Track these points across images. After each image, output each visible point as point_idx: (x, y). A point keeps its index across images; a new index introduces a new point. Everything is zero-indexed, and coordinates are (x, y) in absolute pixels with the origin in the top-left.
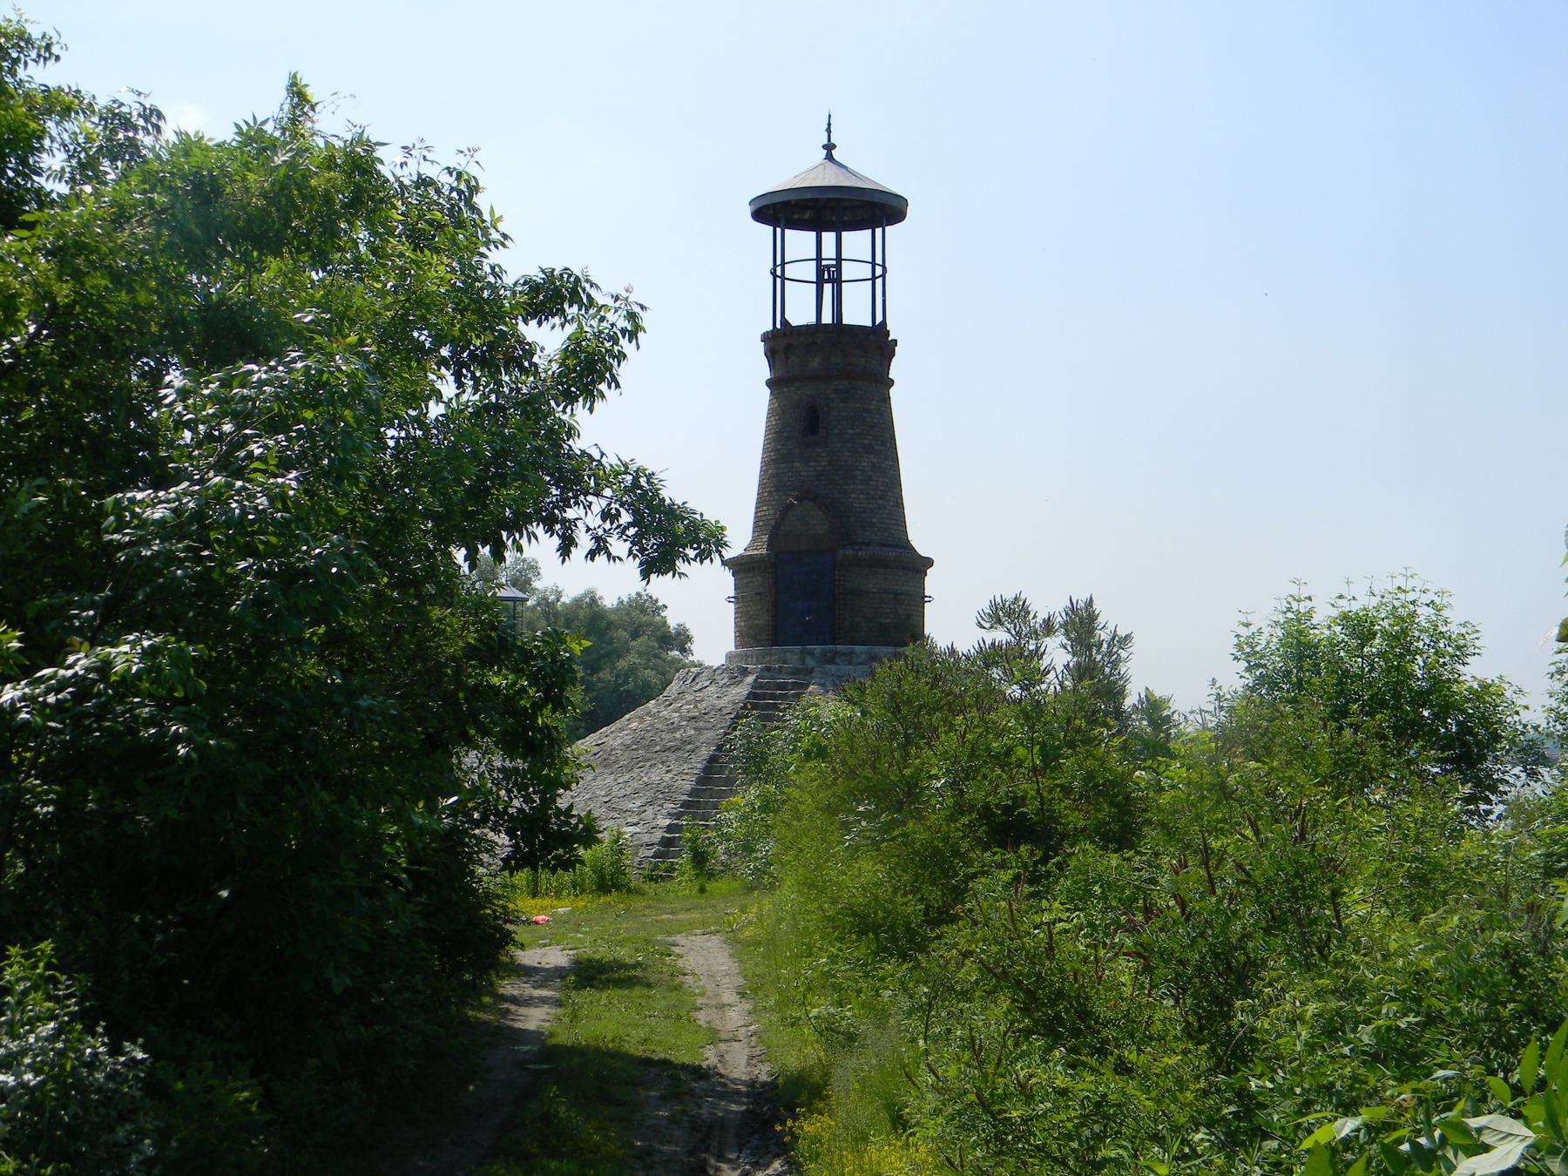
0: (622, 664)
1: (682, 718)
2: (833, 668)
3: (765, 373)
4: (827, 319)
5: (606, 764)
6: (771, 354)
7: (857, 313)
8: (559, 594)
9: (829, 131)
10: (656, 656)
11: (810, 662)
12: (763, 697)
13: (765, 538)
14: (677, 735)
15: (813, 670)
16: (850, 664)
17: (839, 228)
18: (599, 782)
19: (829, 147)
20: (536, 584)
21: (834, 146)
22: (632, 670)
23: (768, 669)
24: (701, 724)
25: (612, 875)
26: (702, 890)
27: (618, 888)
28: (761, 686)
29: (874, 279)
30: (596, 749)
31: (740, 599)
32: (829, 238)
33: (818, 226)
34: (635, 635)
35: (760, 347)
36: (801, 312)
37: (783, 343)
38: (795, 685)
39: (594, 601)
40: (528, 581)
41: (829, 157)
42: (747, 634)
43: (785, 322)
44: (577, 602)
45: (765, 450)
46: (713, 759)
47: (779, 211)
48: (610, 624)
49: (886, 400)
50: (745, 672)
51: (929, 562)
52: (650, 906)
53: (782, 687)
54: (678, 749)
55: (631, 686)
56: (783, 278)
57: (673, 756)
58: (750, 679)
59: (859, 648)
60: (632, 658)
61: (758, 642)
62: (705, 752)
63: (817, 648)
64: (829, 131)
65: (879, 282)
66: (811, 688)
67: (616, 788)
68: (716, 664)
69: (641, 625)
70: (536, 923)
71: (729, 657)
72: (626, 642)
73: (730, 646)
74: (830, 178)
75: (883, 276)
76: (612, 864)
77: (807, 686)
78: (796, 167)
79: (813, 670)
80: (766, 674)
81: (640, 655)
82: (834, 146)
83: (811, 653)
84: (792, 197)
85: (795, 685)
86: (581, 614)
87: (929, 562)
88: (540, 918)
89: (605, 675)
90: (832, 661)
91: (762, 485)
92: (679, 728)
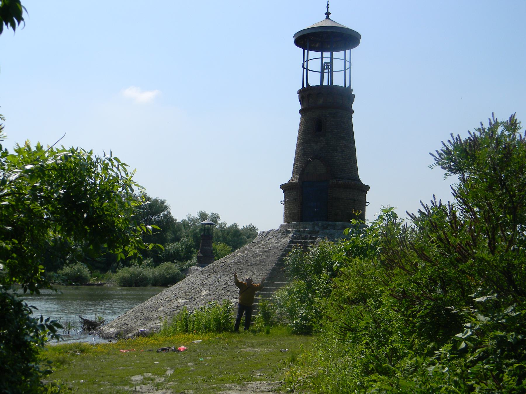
1: (260, 251)
2: (327, 231)
3: (299, 107)
4: (325, 83)
5: (226, 270)
6: (301, 100)
7: (338, 81)
8: (225, 225)
9: (328, 7)
11: (317, 229)
12: (296, 243)
13: (298, 176)
14: (258, 259)
15: (318, 232)
16: (334, 229)
17: (332, 50)
18: (222, 278)
19: (328, 14)
20: (219, 222)
21: (330, 14)
23: (298, 231)
24: (269, 254)
25: (224, 323)
26: (268, 333)
27: (226, 329)
28: (296, 238)
29: (345, 70)
30: (222, 264)
31: (301, 123)
32: (327, 55)
33: (321, 49)
35: (297, 96)
36: (314, 80)
37: (307, 94)
38: (310, 238)
39: (236, 226)
40: (216, 221)
41: (328, 18)
42: (289, 216)
43: (308, 85)
44: (231, 227)
45: (298, 139)
46: (273, 270)
47: (308, 40)
48: (241, 234)
49: (351, 118)
50: (288, 232)
51: (367, 188)
52: (240, 341)
53: (305, 238)
54: (258, 265)
56: (308, 70)
57: (256, 268)
58: (291, 235)
59: (338, 223)
61: (294, 220)
62: (270, 266)
63: (320, 223)
64: (328, 7)
65: (348, 72)
66: (318, 239)
67: (229, 282)
68: (276, 227)
69: (250, 235)
70: (179, 351)
71: (281, 226)
72: (245, 240)
73: (282, 222)
74: (328, 24)
75: (350, 68)
76: (224, 317)
77: (316, 238)
78: (314, 19)
79: (318, 232)
80: (298, 233)
82: (330, 14)
83: (317, 225)
84: (313, 31)
85: (310, 238)
87: (367, 188)
88: (182, 347)
90: (327, 228)
91: (297, 154)
92: (258, 255)
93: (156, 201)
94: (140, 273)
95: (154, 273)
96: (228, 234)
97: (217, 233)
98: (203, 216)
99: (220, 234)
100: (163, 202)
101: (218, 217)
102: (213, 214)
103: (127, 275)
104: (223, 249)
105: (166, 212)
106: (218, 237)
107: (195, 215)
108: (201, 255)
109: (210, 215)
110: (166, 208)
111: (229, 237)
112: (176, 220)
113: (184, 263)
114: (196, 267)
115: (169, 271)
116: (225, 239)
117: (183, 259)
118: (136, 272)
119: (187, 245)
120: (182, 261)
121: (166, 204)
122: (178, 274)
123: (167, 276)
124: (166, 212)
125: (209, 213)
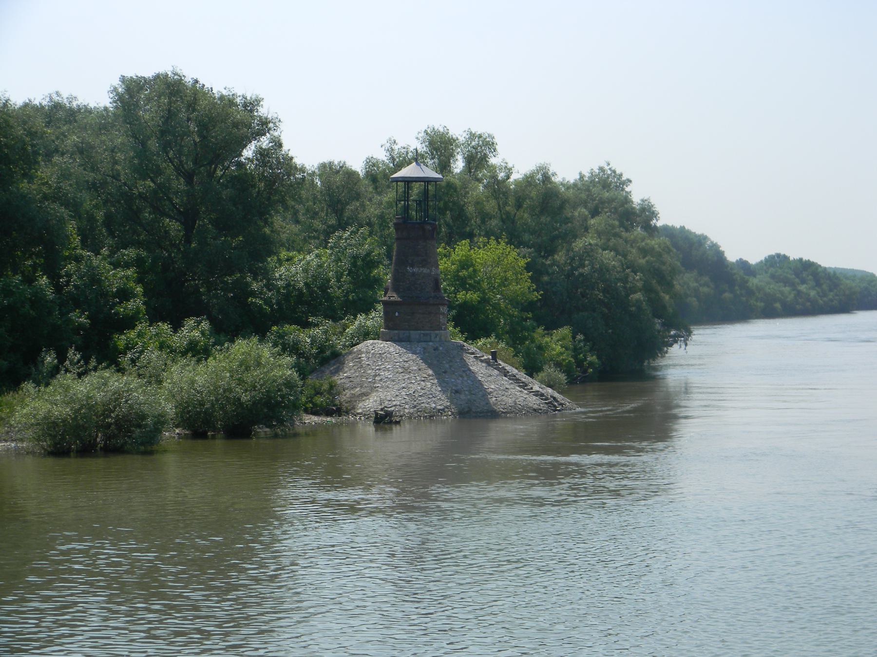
0: (579, 244)
8: (509, 172)
10: (616, 235)
20: (493, 161)
22: (589, 252)
34: (595, 213)
39: (546, 178)
40: (485, 158)
44: (529, 181)
48: (564, 202)
55: (586, 270)
60: (590, 239)
69: (602, 202)
72: (585, 220)
81: (599, 234)
86: (534, 194)
89: (560, 257)
93: (228, 102)
94: (118, 395)
95: (193, 382)
96: (519, 206)
98: (440, 146)
99: (491, 206)
100: (251, 106)
101: (489, 144)
102: (472, 136)
104: (498, 263)
105: (265, 142)
106: (485, 217)
107: (412, 141)
108: (395, 297)
109: (462, 139)
110: (265, 126)
111: (525, 217)
113: (345, 327)
114: (381, 345)
115: (248, 378)
116: (508, 220)
118: (99, 396)
119: (355, 258)
120: (335, 319)
121: (263, 111)
122: (289, 384)
123: (245, 398)
124: (265, 142)
125: (458, 132)
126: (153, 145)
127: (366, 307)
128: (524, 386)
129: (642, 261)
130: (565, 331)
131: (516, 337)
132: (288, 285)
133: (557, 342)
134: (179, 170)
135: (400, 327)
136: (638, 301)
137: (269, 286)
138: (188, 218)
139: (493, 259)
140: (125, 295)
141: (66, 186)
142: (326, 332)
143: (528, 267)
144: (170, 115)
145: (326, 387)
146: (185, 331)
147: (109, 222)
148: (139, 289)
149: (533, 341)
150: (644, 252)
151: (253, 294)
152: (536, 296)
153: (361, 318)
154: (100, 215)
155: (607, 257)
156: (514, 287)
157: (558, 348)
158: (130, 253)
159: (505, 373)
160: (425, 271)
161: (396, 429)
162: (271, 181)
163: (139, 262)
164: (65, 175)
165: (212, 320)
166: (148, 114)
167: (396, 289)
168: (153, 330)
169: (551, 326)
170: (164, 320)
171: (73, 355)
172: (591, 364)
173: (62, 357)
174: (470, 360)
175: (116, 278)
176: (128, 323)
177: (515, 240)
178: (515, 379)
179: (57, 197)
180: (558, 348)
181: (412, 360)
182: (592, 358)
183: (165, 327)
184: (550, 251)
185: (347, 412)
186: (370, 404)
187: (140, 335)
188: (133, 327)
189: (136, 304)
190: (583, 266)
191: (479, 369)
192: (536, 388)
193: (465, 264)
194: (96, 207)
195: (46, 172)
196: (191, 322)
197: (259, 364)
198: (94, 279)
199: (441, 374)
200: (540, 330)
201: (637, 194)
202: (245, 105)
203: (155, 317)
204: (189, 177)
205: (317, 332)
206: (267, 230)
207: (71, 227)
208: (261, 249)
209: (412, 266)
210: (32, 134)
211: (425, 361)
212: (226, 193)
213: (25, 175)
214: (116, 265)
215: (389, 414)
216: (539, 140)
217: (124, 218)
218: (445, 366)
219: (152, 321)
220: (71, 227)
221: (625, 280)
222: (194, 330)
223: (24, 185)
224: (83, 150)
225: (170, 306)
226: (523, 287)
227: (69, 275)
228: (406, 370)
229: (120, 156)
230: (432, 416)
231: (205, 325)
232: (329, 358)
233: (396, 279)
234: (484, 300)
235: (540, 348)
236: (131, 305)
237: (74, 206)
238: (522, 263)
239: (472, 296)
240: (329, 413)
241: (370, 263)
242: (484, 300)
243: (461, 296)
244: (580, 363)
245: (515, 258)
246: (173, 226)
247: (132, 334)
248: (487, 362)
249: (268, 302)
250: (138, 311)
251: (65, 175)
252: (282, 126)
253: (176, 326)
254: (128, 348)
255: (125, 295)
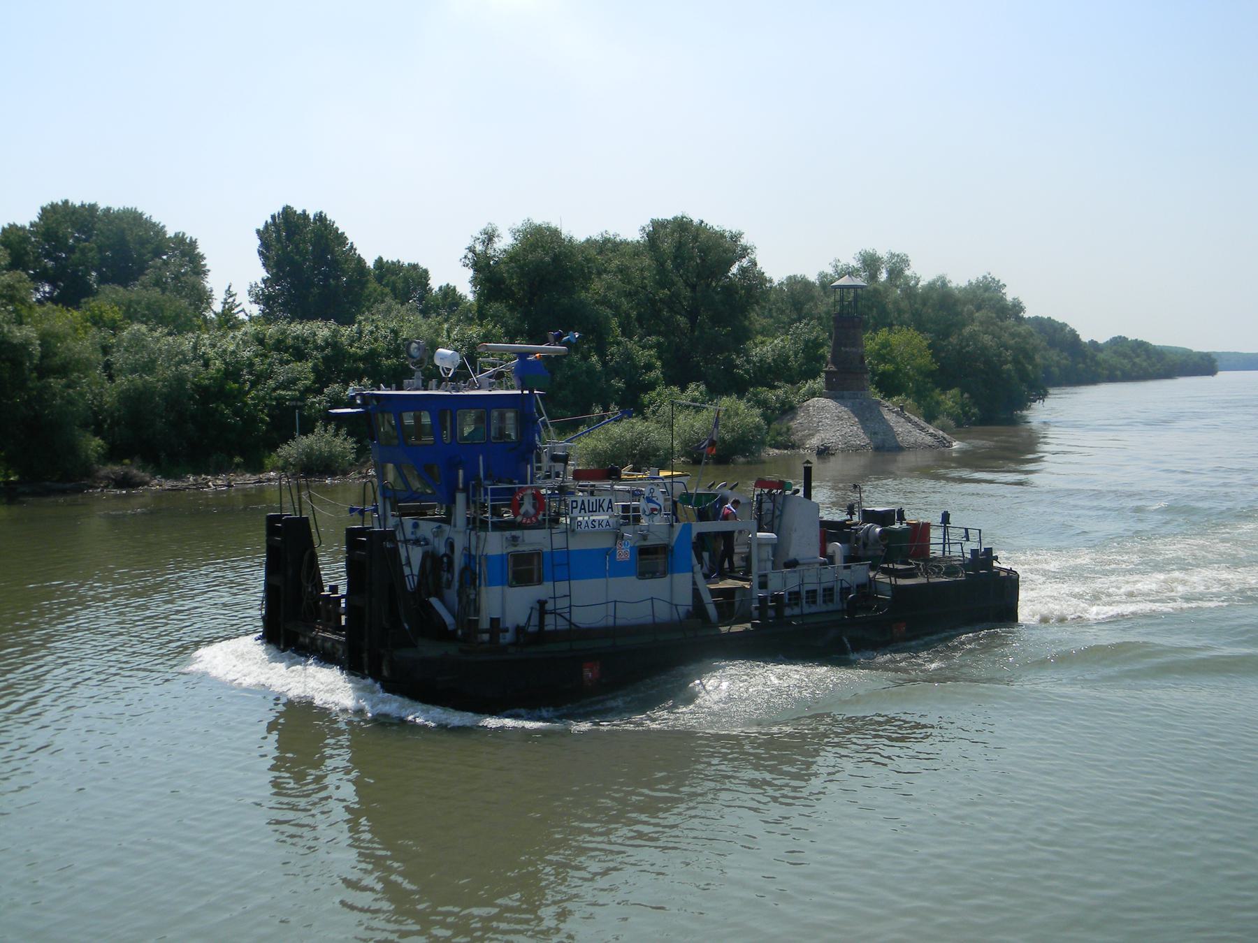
20: (907, 273)
22: (973, 336)
34: (979, 308)
39: (944, 284)
40: (902, 271)
44: (931, 287)
69: (983, 301)
72: (972, 313)
81: (981, 323)
86: (935, 296)
89: (954, 340)
95: (693, 426)
96: (924, 304)
97: (896, 302)
98: (870, 263)
99: (904, 304)
100: (735, 238)
101: (905, 261)
102: (893, 255)
103: (603, 446)
104: (908, 344)
106: (900, 312)
107: (851, 260)
108: (833, 368)
110: (745, 251)
112: (771, 281)
113: (800, 388)
114: (823, 401)
117: (794, 378)
119: (806, 342)
120: (793, 383)
121: (743, 242)
122: (758, 428)
123: (727, 437)
124: (745, 262)
125: (883, 253)
126: (669, 265)
127: (813, 375)
128: (922, 429)
129: (1012, 342)
130: (955, 391)
131: (920, 395)
132: (761, 361)
133: (949, 399)
134: (687, 284)
135: (835, 390)
136: (1009, 370)
137: (748, 362)
138: (692, 315)
139: (906, 343)
140: (649, 367)
141: (610, 294)
142: (786, 392)
143: (930, 347)
144: (680, 246)
145: (784, 429)
146: (689, 391)
147: (640, 319)
148: (659, 364)
149: (932, 398)
150: (1013, 335)
151: (737, 367)
152: (935, 367)
153: (810, 382)
154: (634, 314)
155: (987, 339)
156: (919, 361)
157: (950, 403)
158: (654, 339)
159: (910, 421)
160: (854, 350)
161: (832, 458)
162: (750, 289)
163: (658, 345)
164: (610, 288)
165: (707, 384)
166: (667, 245)
167: (834, 363)
168: (667, 391)
169: (946, 388)
170: (675, 385)
171: (614, 408)
172: (974, 415)
173: (606, 409)
174: (885, 412)
175: (643, 356)
176: (651, 386)
177: (921, 327)
178: (916, 425)
179: (605, 302)
180: (950, 403)
181: (844, 411)
182: (975, 410)
183: (676, 389)
184: (947, 336)
185: (799, 448)
186: (815, 441)
187: (659, 394)
188: (654, 389)
189: (656, 374)
190: (968, 345)
191: (891, 418)
192: (931, 431)
193: (885, 345)
194: (631, 308)
195: (597, 285)
196: (693, 386)
197: (737, 414)
198: (628, 357)
199: (863, 422)
200: (938, 391)
201: (1010, 295)
202: (731, 238)
203: (669, 381)
204: (693, 287)
205: (780, 392)
206: (747, 323)
207: (614, 322)
208: (742, 336)
209: (845, 346)
210: (588, 260)
211: (853, 412)
212: (717, 298)
213: (583, 288)
214: (644, 348)
215: (827, 448)
216: (941, 258)
217: (649, 315)
218: (867, 415)
219: (667, 385)
220: (614, 322)
221: (999, 355)
222: (695, 390)
223: (583, 294)
224: (622, 270)
225: (680, 375)
226: (926, 360)
227: (612, 355)
228: (840, 419)
229: (646, 274)
230: (857, 449)
231: (703, 388)
232: (788, 410)
233: (833, 356)
234: (898, 370)
235: (938, 403)
236: (653, 374)
237: (616, 309)
238: (925, 343)
239: (889, 367)
240: (786, 448)
241: (817, 344)
242: (898, 370)
243: (881, 367)
244: (965, 414)
245: (920, 341)
246: (682, 320)
247: (654, 394)
248: (896, 412)
249: (747, 372)
250: (658, 378)
251: (610, 288)
252: (757, 251)
253: (683, 389)
254: (650, 403)
255: (649, 367)
